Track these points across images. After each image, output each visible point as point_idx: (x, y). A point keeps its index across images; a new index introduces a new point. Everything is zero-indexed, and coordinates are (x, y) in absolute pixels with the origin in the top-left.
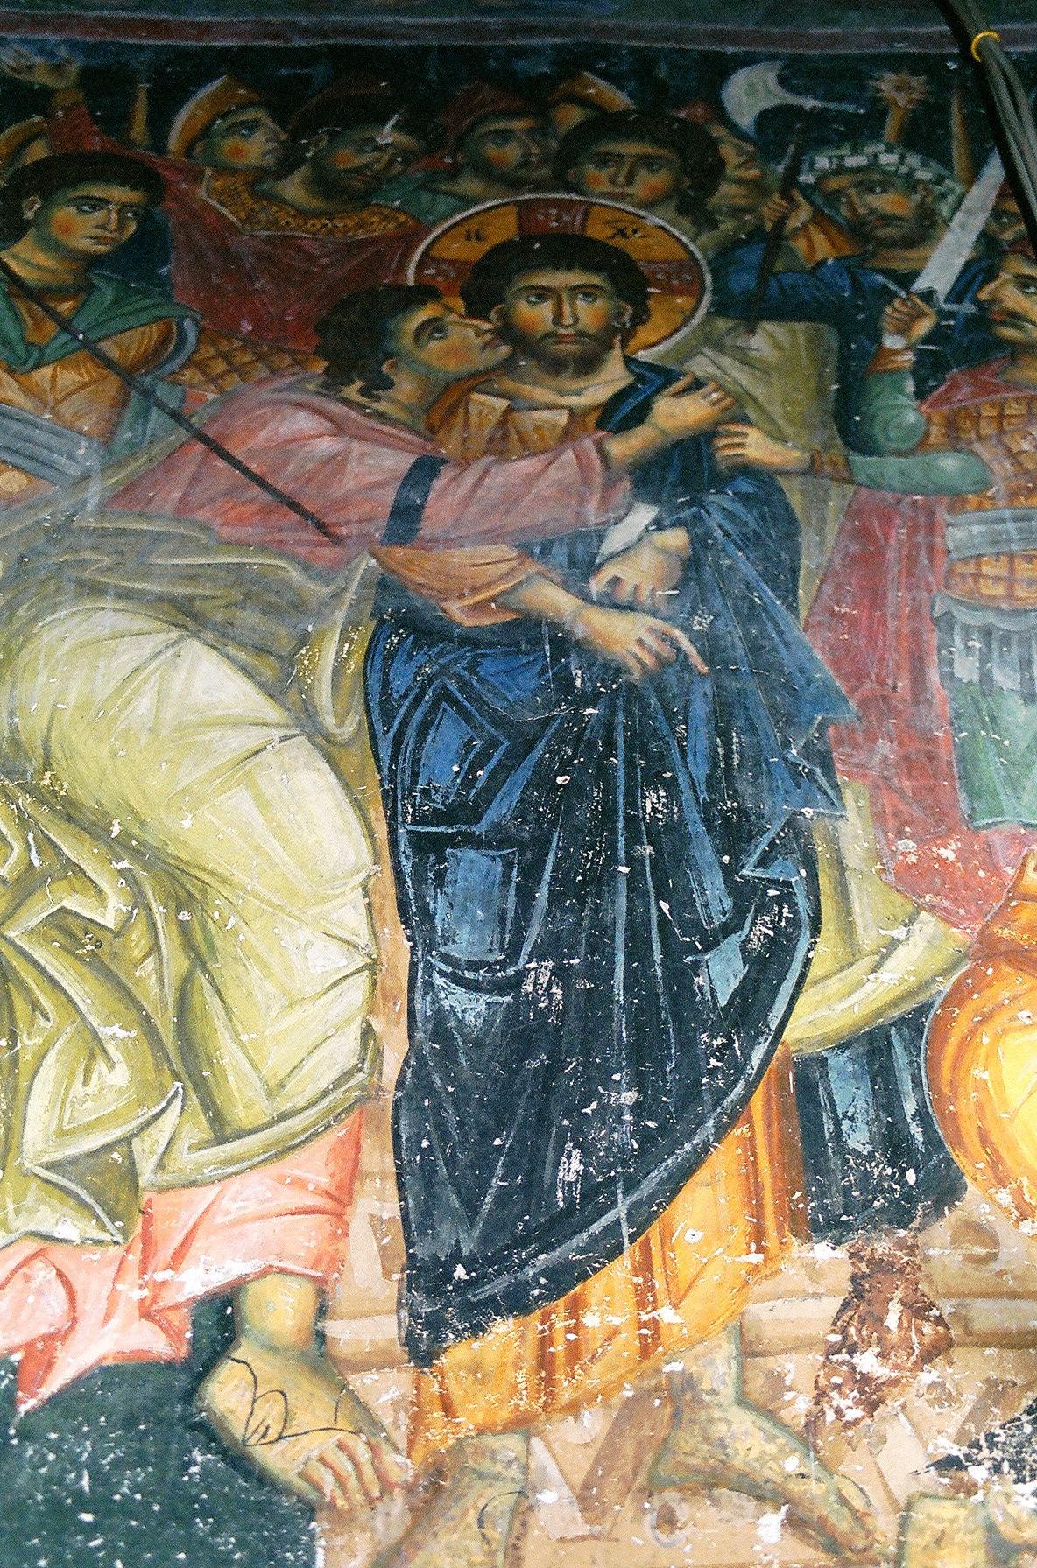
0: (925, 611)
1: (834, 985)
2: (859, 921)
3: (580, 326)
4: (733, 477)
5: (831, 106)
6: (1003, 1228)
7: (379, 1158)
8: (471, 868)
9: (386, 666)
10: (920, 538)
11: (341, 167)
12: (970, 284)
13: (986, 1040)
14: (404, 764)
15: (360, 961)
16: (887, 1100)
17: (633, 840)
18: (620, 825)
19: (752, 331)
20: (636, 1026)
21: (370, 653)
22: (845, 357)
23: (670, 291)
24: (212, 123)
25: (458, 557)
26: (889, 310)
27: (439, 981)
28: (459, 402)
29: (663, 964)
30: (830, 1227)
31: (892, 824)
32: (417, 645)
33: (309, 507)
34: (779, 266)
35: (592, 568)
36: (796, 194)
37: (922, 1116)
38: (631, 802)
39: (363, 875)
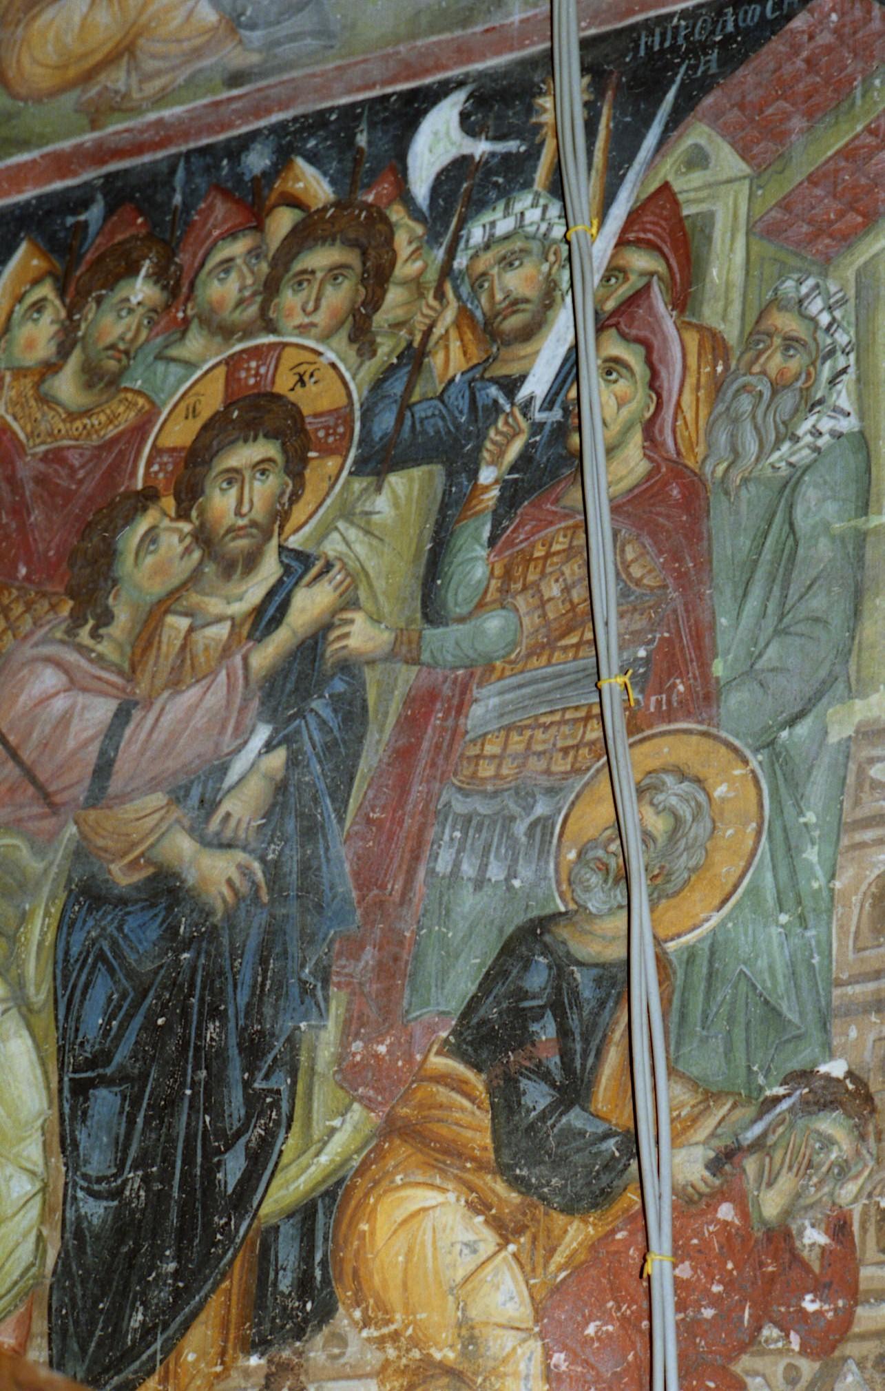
0: (432, 807)
1: (293, 1170)
2: (315, 1116)
3: (253, 515)
4: (332, 676)
5: (501, 147)
6: (352, 1335)
7: (40, 1325)
8: (105, 1101)
9: (69, 934)
10: (450, 723)
11: (101, 345)
12: (564, 381)
13: (372, 1200)
14: (72, 1024)
15: (38, 1185)
16: (307, 1256)
17: (196, 1068)
18: (191, 1054)
19: (379, 489)
20: (181, 1216)
21: (59, 928)
22: (444, 507)
23: (327, 451)
24: (11, 312)
25: (129, 810)
26: (492, 433)
27: (80, 1194)
28: (156, 628)
29: (202, 1166)
30: (260, 1345)
31: (353, 1028)
32: (90, 911)
33: (42, 777)
34: (414, 399)
35: (216, 805)
36: (448, 288)
37: (324, 1263)
38: (199, 1036)
39: (40, 1122)
